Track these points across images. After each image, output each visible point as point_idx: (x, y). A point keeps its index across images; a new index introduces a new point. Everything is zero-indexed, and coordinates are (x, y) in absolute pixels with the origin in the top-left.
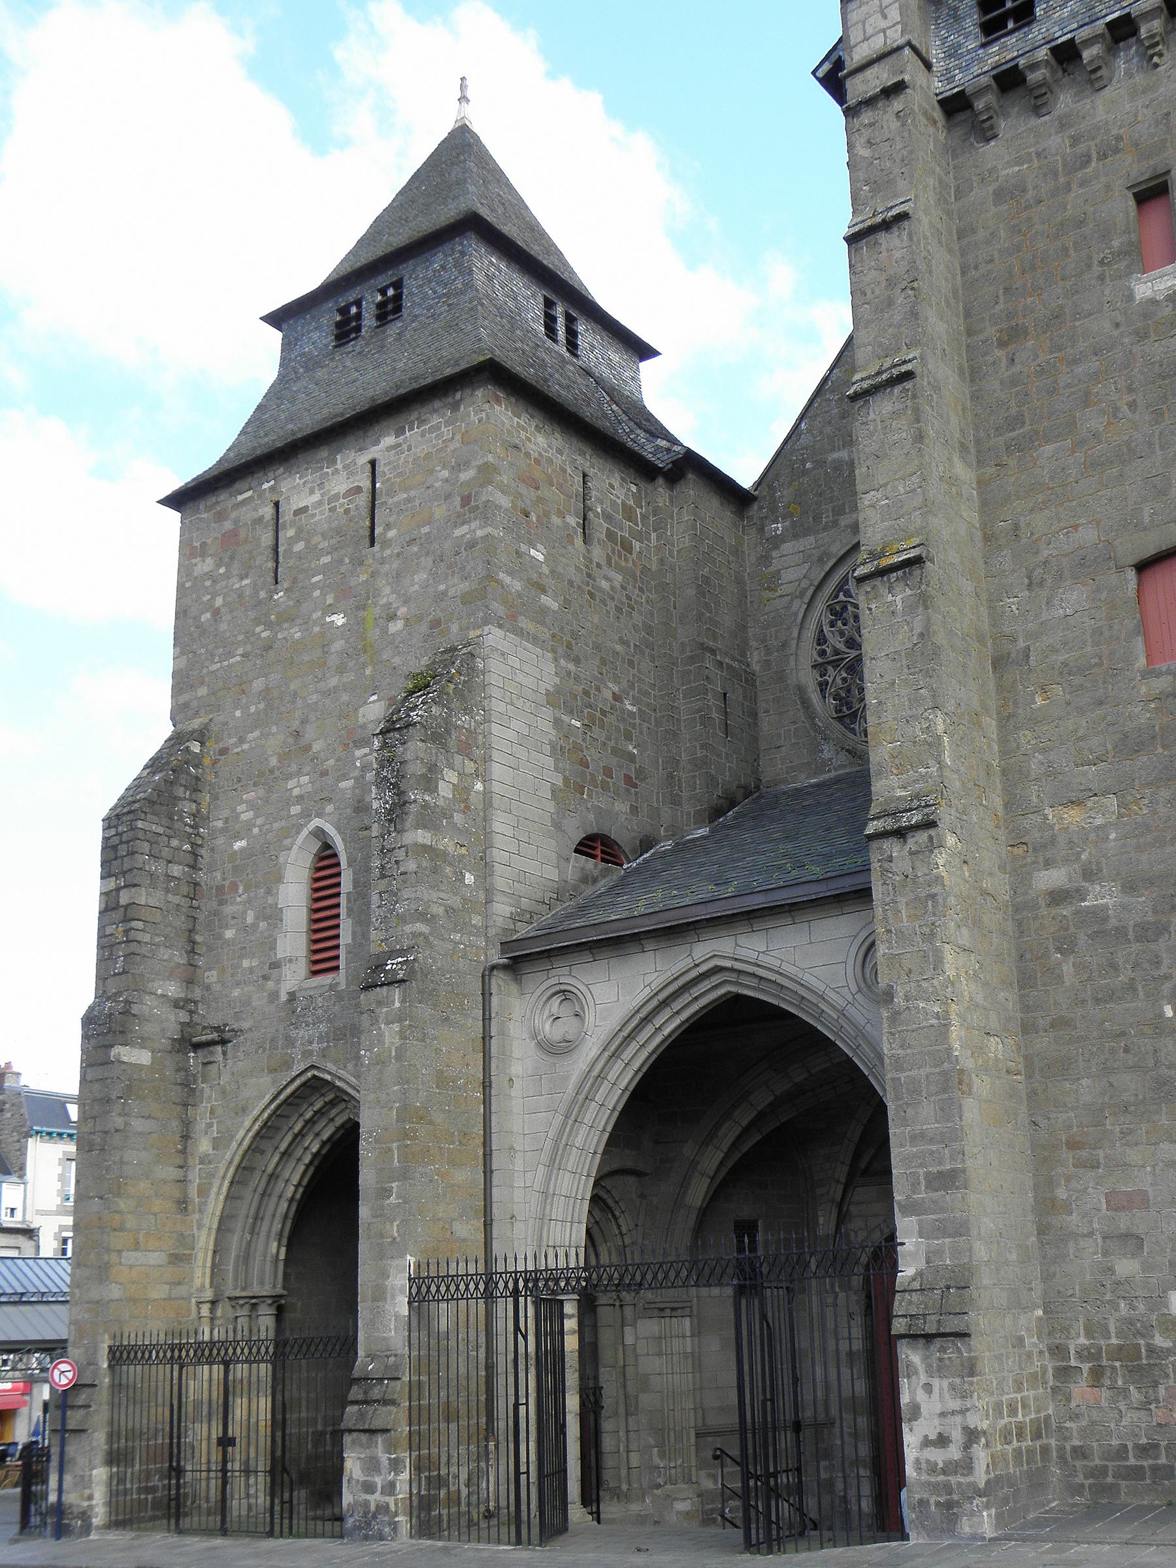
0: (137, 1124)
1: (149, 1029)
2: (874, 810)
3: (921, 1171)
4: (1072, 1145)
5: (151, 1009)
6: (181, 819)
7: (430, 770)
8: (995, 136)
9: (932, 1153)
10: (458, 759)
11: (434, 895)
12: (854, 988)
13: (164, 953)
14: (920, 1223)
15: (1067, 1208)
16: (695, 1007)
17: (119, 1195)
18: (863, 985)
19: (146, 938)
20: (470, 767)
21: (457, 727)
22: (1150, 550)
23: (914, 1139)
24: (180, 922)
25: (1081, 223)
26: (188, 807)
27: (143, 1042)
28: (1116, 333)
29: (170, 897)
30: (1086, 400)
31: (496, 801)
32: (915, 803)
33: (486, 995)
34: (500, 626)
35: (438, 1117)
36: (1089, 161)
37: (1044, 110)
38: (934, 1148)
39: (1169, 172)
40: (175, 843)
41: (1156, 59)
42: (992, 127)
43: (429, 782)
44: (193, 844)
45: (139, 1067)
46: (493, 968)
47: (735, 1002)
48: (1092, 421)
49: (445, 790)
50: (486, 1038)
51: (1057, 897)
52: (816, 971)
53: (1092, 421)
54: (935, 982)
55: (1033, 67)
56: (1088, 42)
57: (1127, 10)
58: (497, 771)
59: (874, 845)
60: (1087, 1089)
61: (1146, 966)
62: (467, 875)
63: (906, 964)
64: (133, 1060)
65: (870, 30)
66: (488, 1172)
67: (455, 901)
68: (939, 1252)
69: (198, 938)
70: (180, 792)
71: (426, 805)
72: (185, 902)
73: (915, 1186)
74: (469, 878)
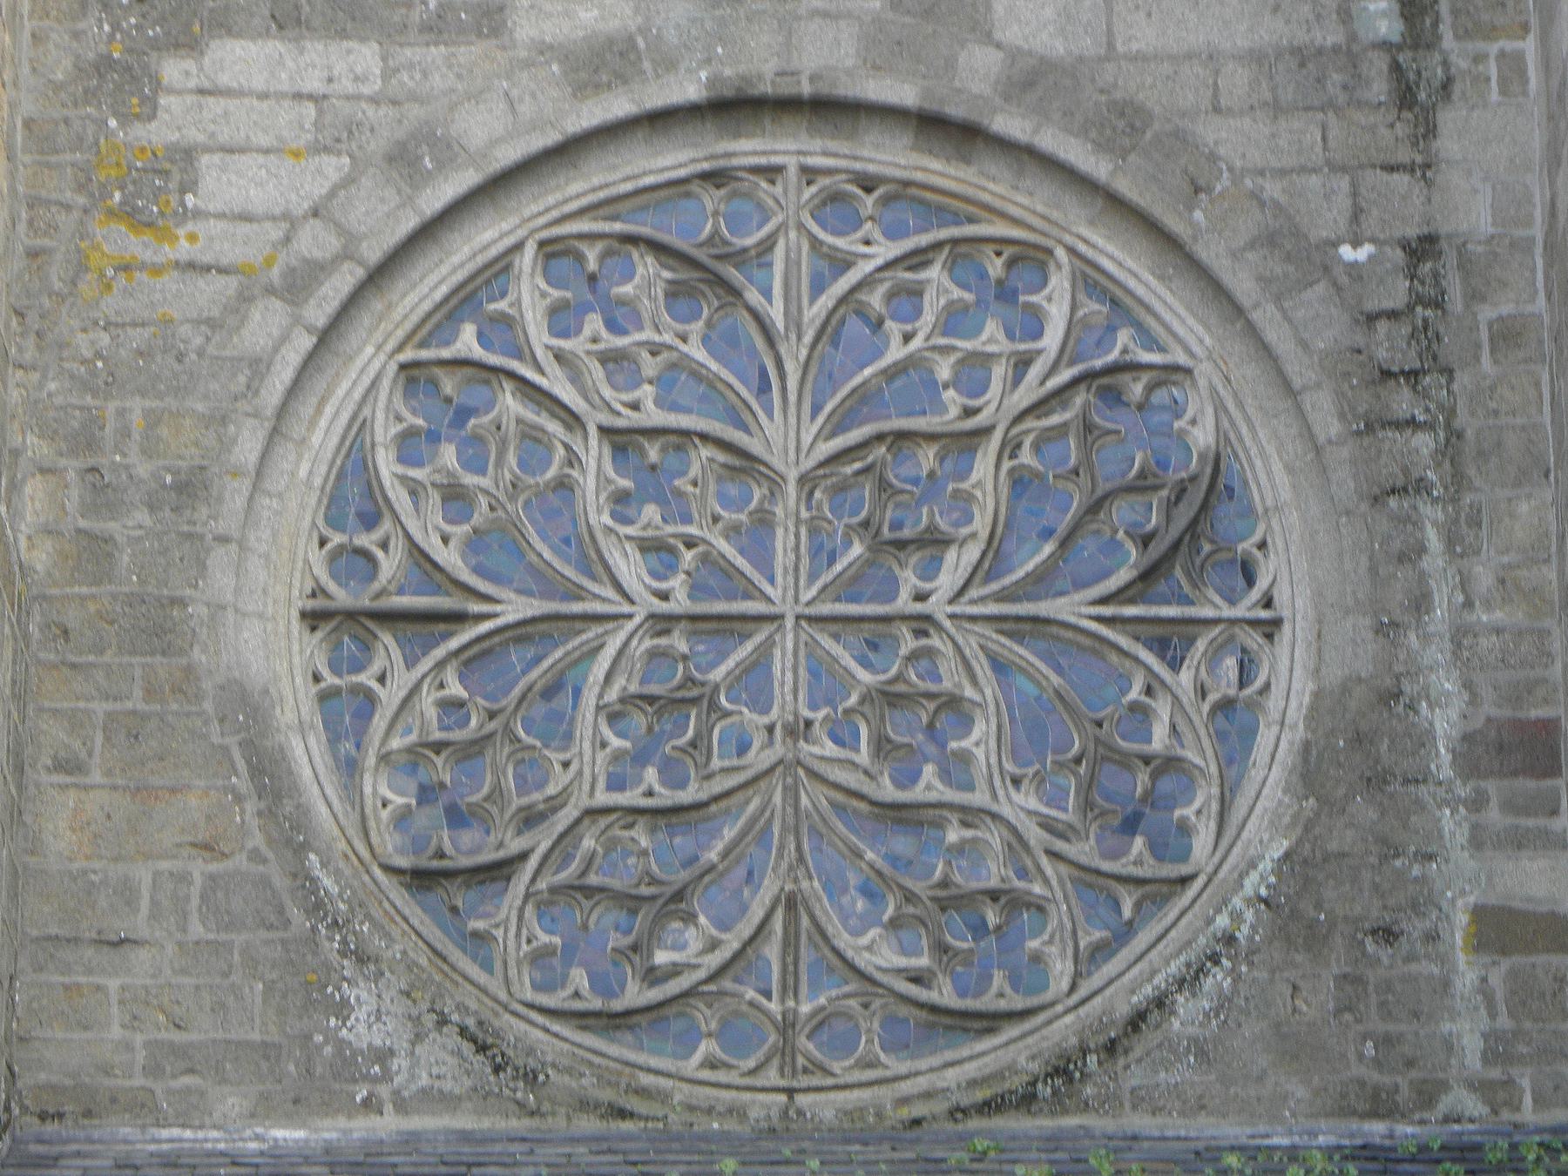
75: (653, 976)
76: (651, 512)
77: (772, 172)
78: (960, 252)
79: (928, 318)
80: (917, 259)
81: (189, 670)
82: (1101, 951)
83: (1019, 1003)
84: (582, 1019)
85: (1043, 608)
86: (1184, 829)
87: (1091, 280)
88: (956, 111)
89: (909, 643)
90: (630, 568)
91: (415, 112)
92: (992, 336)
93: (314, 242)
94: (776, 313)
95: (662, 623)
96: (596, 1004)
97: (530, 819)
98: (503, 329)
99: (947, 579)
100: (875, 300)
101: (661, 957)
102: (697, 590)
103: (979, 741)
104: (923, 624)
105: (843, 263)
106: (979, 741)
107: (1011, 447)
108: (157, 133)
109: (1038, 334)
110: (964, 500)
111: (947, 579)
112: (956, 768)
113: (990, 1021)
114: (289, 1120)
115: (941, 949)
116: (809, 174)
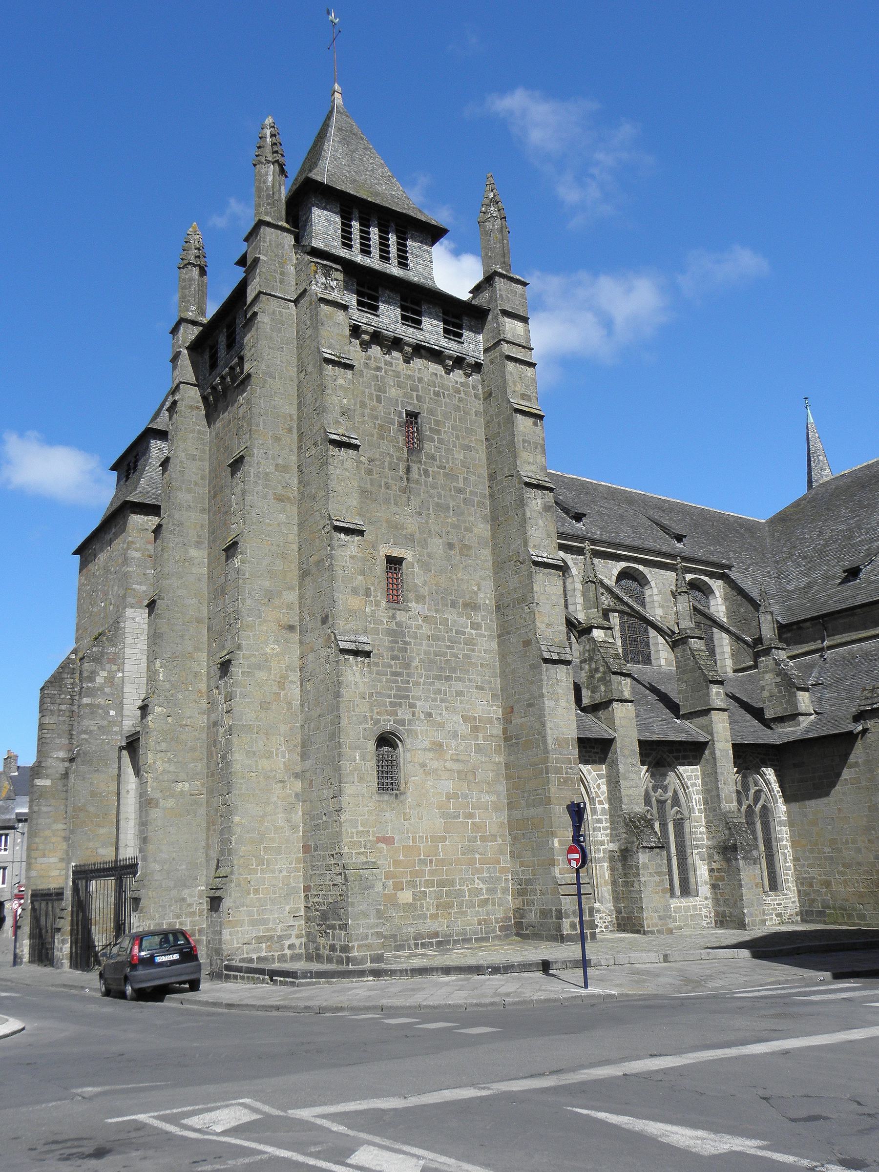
0: (44, 809)
1: (49, 771)
5: (51, 763)
6: (66, 686)
7: (91, 673)
10: (108, 666)
11: (92, 722)
13: (57, 741)
17: (36, 837)
19: (49, 736)
20: (114, 668)
21: (107, 653)
24: (66, 727)
26: (69, 681)
27: (47, 777)
29: (60, 718)
31: (126, 680)
33: (120, 758)
34: (132, 607)
35: (91, 809)
40: (62, 696)
43: (91, 679)
44: (71, 696)
45: (46, 787)
46: (121, 748)
49: (99, 680)
50: (119, 776)
58: (127, 667)
62: (111, 712)
64: (42, 784)
66: (118, 829)
67: (105, 723)
69: (74, 733)
70: (65, 676)
71: (88, 688)
72: (67, 719)
74: (112, 713)
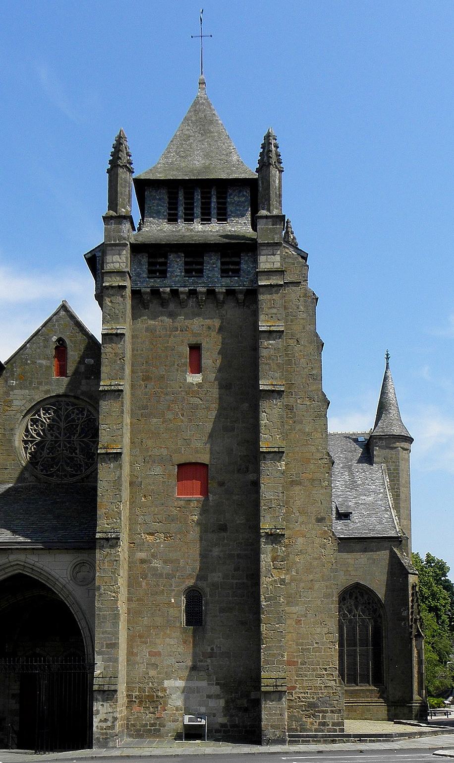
2: (98, 529)
3: (105, 642)
4: (140, 637)
8: (148, 309)
9: (108, 637)
12: (69, 579)
14: (103, 658)
15: (136, 655)
16: (5, 576)
18: (72, 578)
22: (183, 461)
23: (103, 633)
25: (173, 350)
28: (180, 390)
30: (169, 409)
32: (112, 531)
36: (177, 330)
37: (165, 307)
38: (109, 636)
39: (201, 344)
41: (201, 306)
42: (148, 305)
47: (20, 576)
48: (169, 415)
51: (143, 561)
52: (57, 571)
53: (169, 415)
54: (114, 587)
55: (164, 293)
56: (182, 293)
57: (195, 288)
59: (98, 541)
60: (146, 621)
61: (168, 586)
63: (105, 580)
65: (114, 260)
68: (108, 667)
73: (102, 647)
75: (50, 471)
76: (51, 431)
77: (62, 401)
78: (78, 409)
79: (75, 414)
80: (74, 409)
81: (12, 445)
82: (87, 469)
83: (80, 473)
84: (44, 475)
85: (83, 439)
86: (95, 458)
87: (88, 411)
88: (77, 396)
89: (72, 442)
90: (49, 436)
91: (32, 397)
92: (80, 416)
93: (23, 408)
94: (62, 414)
95: (52, 441)
96: (45, 473)
97: (41, 458)
98: (39, 416)
99: (76, 437)
100: (71, 412)
101: (51, 469)
102: (55, 438)
103: (77, 451)
104: (73, 441)
105: (68, 409)
106: (77, 451)
107: (81, 426)
108: (10, 398)
109: (84, 415)
110: (77, 431)
111: (76, 437)
112: (76, 454)
113: (77, 475)
114: (20, 483)
115: (74, 469)
116: (65, 401)
